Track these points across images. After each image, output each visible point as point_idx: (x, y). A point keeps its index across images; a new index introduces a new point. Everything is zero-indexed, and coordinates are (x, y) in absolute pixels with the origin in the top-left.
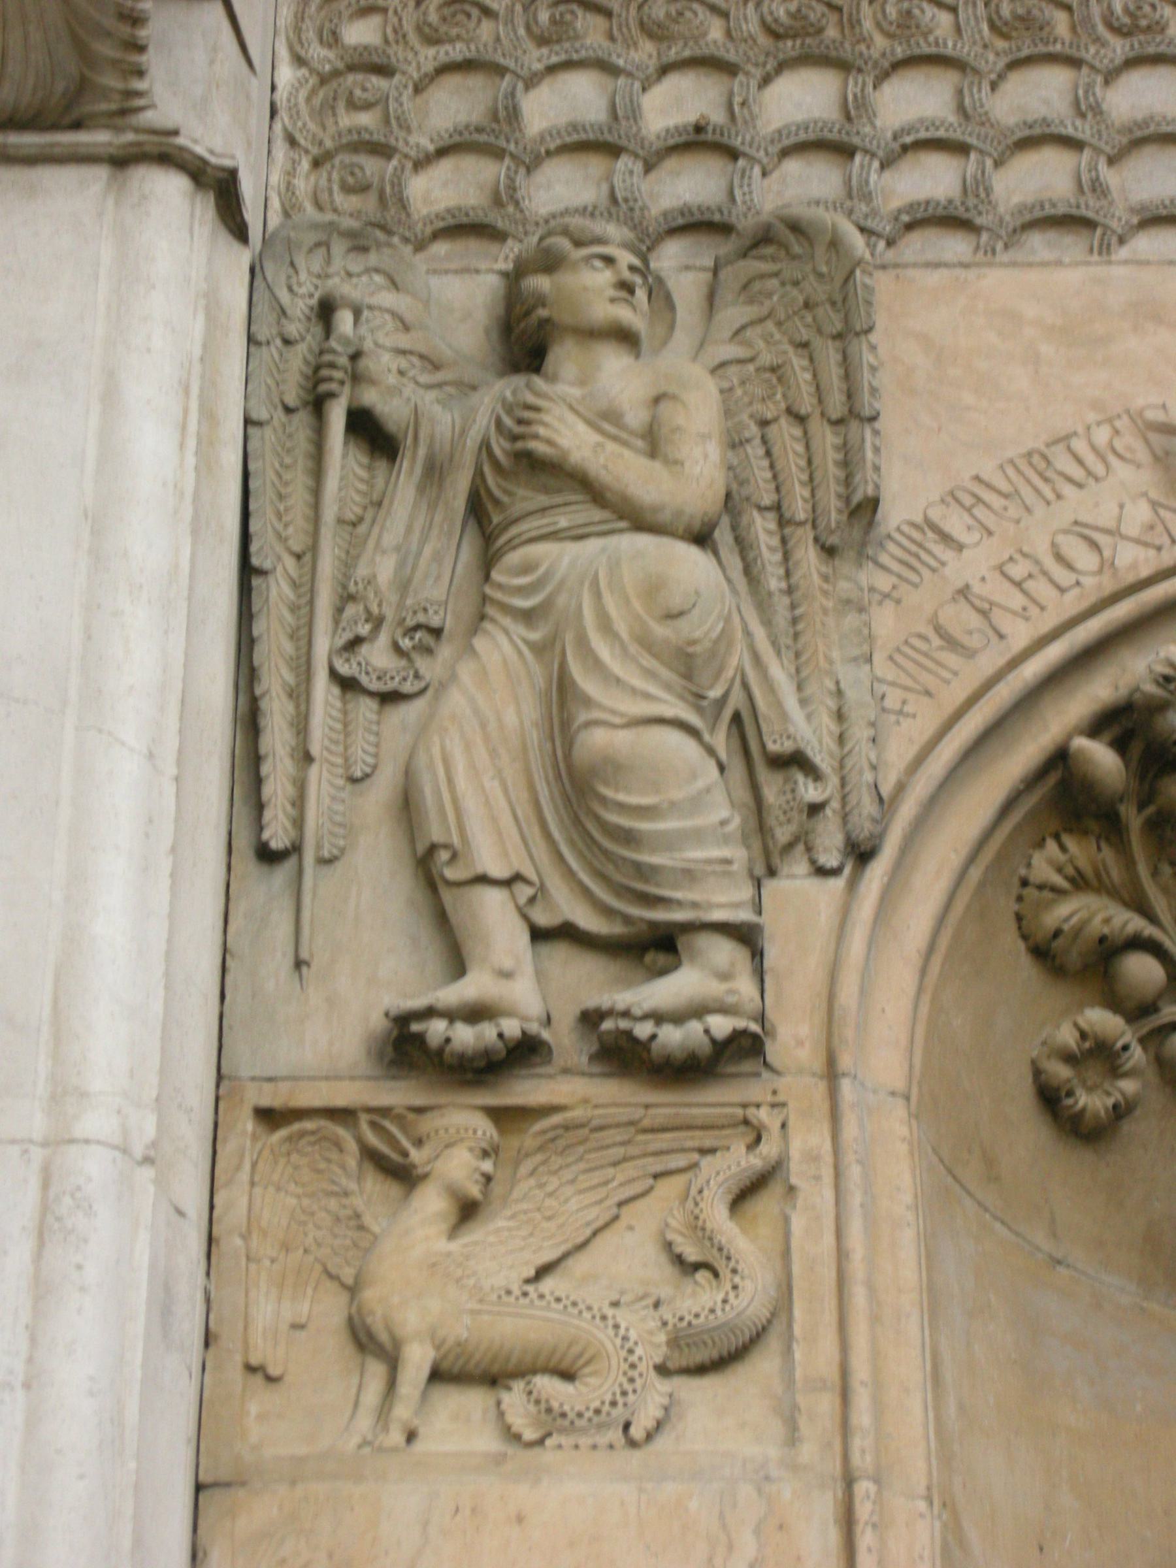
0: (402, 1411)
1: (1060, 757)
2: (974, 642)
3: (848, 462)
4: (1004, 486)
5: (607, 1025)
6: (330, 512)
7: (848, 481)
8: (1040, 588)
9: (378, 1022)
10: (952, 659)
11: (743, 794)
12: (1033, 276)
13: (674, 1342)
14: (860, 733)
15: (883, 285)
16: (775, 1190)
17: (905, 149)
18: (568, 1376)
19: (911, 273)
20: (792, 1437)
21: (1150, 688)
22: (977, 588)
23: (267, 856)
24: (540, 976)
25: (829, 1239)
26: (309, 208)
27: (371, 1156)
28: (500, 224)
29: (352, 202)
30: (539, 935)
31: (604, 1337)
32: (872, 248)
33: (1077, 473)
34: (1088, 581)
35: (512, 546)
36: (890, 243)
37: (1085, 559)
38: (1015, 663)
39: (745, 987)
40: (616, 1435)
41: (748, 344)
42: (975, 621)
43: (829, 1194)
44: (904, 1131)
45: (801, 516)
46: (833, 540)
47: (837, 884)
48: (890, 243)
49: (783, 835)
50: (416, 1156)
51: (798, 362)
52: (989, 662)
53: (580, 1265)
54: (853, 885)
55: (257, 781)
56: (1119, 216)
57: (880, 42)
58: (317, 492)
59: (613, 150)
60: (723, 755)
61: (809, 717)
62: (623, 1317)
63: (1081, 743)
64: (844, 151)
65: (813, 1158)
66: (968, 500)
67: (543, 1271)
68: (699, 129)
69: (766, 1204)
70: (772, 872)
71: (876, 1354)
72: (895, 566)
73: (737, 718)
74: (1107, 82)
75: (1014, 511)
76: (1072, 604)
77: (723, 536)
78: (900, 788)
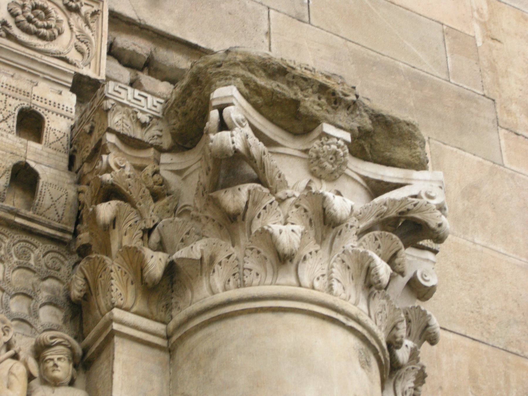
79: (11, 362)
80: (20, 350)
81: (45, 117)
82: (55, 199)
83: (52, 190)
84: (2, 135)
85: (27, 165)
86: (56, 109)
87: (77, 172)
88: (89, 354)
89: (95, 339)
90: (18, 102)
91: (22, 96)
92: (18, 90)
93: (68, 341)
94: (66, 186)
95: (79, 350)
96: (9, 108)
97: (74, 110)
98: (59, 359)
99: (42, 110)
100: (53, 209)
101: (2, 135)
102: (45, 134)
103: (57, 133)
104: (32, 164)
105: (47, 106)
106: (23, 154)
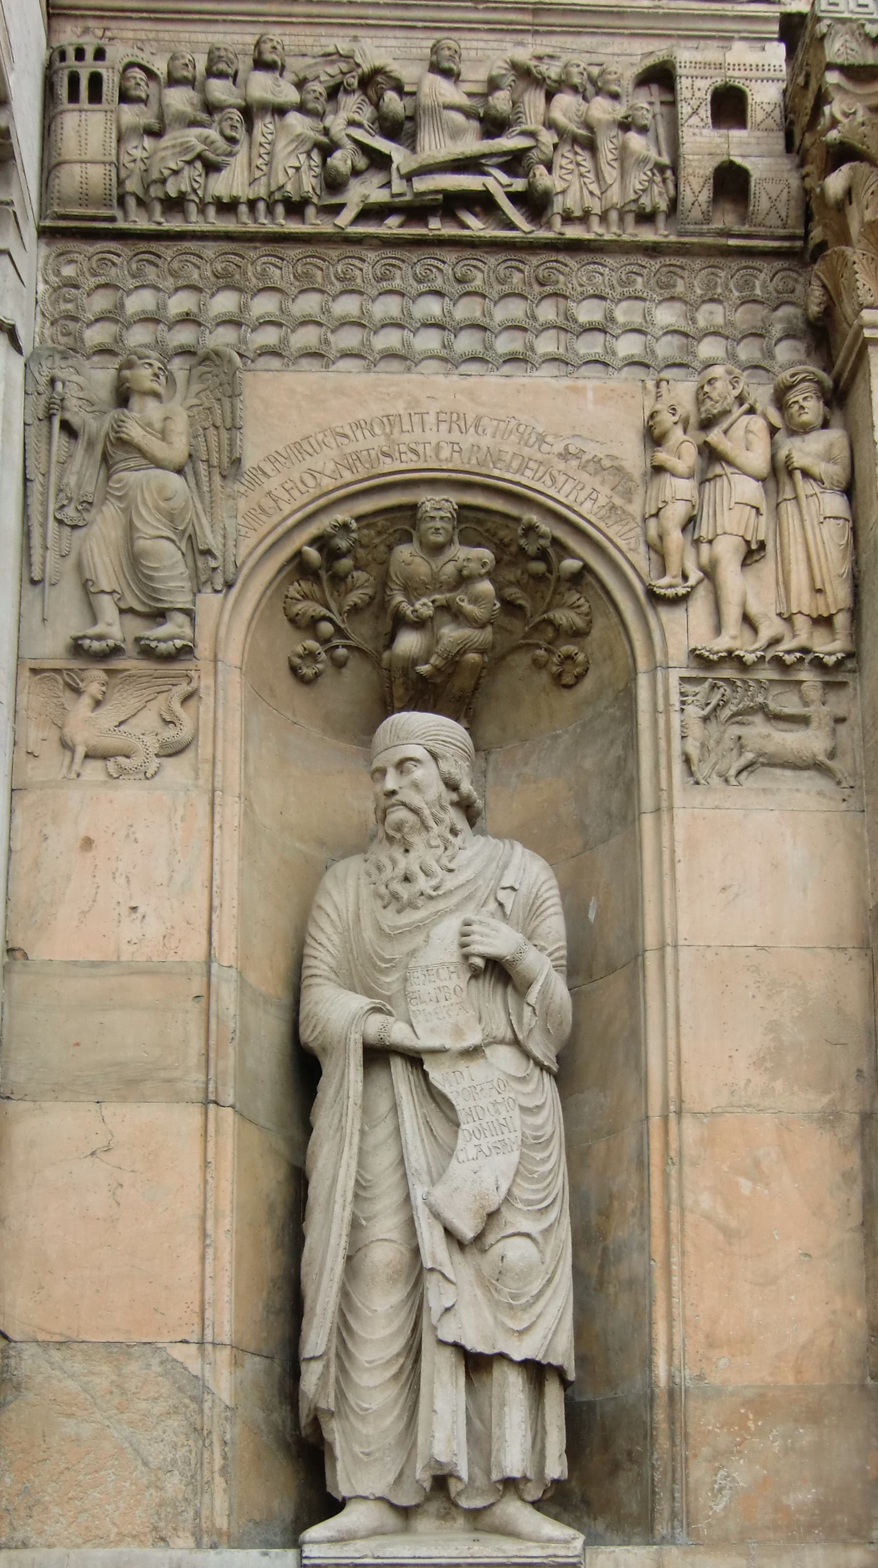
0: (76, 767)
1: (299, 554)
2: (271, 511)
3: (232, 445)
4: (285, 455)
5: (142, 642)
6: (54, 459)
7: (231, 452)
8: (295, 493)
9: (69, 641)
10: (263, 518)
11: (190, 563)
12: (300, 375)
13: (161, 747)
14: (231, 543)
15: (247, 379)
16: (195, 698)
17: (261, 324)
18: (128, 757)
19: (259, 373)
20: (197, 777)
21: (329, 530)
22: (274, 492)
23: (34, 582)
24: (122, 625)
25: (211, 715)
26: (49, 341)
27: (67, 685)
28: (116, 350)
29: (63, 340)
30: (122, 611)
31: (139, 745)
32: (245, 364)
33: (310, 450)
34: (311, 490)
35: (115, 472)
36: (253, 361)
37: (311, 482)
38: (284, 519)
39: (187, 631)
40: (142, 776)
41: (200, 399)
42: (272, 503)
43: (212, 700)
44: (238, 680)
45: (215, 464)
46: (225, 473)
47: (221, 595)
48: (253, 361)
49: (203, 578)
50: (81, 685)
51: (217, 406)
52: (276, 519)
53: (133, 721)
54: (226, 596)
55: (30, 556)
56: (333, 353)
57: (254, 280)
58: (49, 451)
59: (157, 321)
60: (184, 550)
61: (214, 537)
62: (145, 738)
63: (306, 548)
64: (238, 324)
65: (207, 687)
66: (273, 460)
67: (121, 723)
68: (188, 314)
69: (192, 703)
70: (199, 591)
71: (225, 752)
72: (246, 483)
73: (190, 537)
74: (333, 300)
75: (288, 465)
76: (305, 499)
77: (188, 470)
78: (244, 563)
79: (747, 418)
80: (756, 401)
81: (747, 90)
82: (774, 197)
83: (769, 186)
84: (694, 134)
85: (732, 163)
86: (760, 74)
87: (798, 153)
88: (841, 384)
89: (846, 360)
90: (709, 82)
91: (712, 72)
92: (707, 65)
93: (813, 373)
94: (786, 175)
95: (828, 381)
96: (698, 94)
97: (784, 67)
98: (805, 399)
99: (742, 81)
100: (773, 212)
101: (694, 134)
102: (749, 113)
103: (765, 106)
104: (738, 160)
105: (748, 74)
106: (724, 151)
